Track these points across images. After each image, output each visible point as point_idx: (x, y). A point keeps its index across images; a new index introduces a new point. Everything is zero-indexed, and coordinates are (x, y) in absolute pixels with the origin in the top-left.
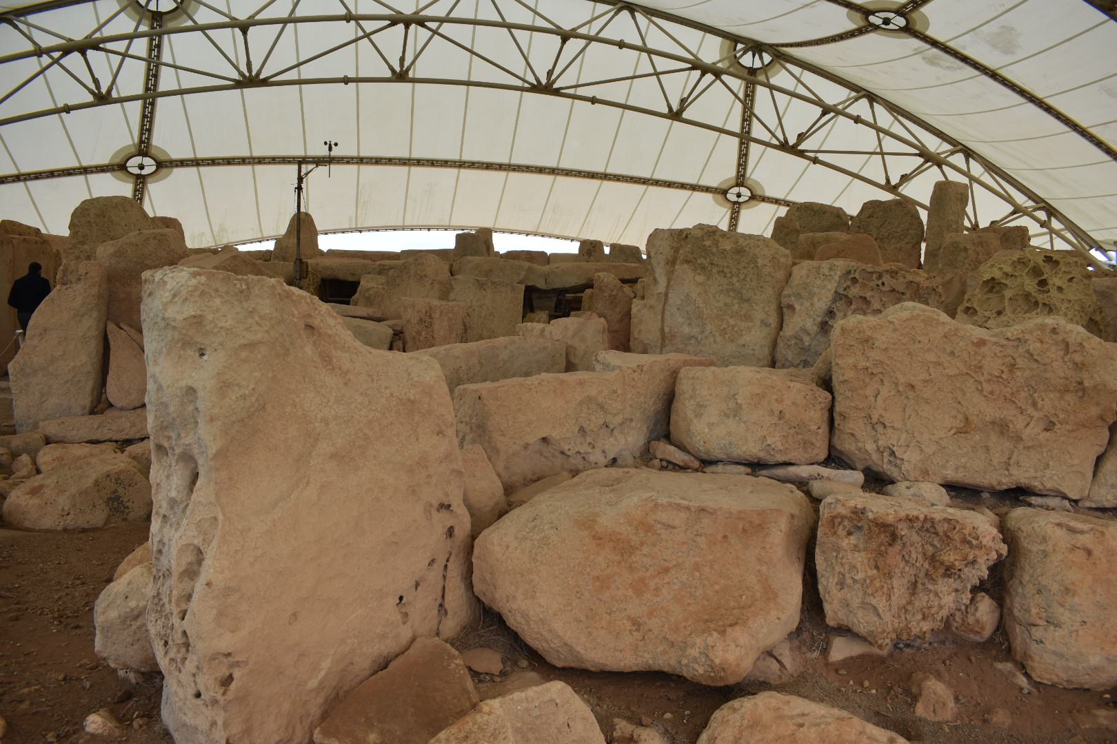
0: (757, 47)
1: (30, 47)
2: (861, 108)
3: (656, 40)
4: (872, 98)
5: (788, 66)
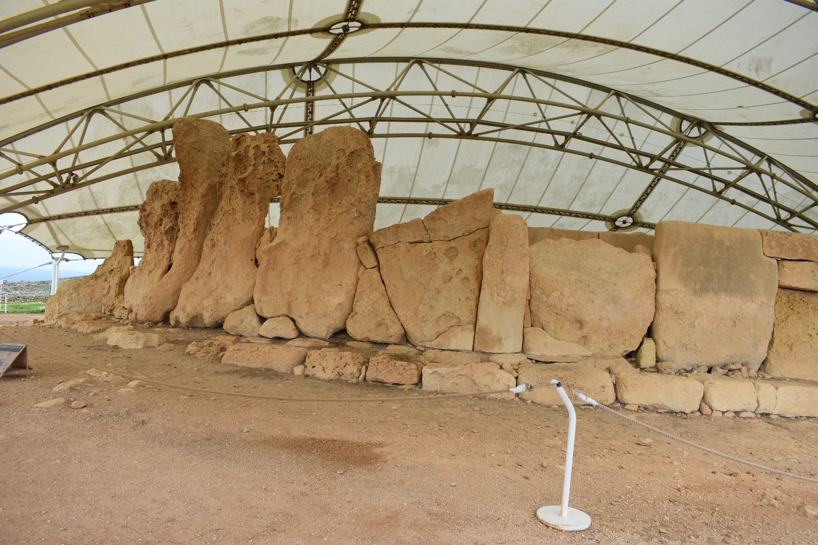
0: (700, 123)
4: (771, 161)
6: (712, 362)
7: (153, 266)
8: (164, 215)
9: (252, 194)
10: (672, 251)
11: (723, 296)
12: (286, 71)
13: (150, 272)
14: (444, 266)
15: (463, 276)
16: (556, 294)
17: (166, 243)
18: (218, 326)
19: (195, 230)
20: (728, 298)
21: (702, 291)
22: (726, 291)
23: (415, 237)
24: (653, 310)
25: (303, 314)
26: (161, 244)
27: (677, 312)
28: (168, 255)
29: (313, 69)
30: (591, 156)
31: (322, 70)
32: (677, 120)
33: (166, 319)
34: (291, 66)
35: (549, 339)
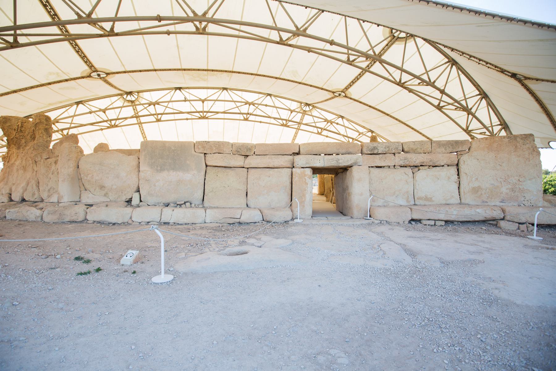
0: (307, 105)
1: (88, 111)
2: (340, 121)
3: (278, 104)
4: (342, 117)
5: (317, 110)
6: (167, 201)
10: (144, 153)
11: (172, 171)
16: (90, 176)
20: (174, 173)
21: (162, 170)
22: (173, 169)
24: (137, 180)
27: (146, 180)
30: (261, 122)
32: (299, 104)
35: (91, 195)
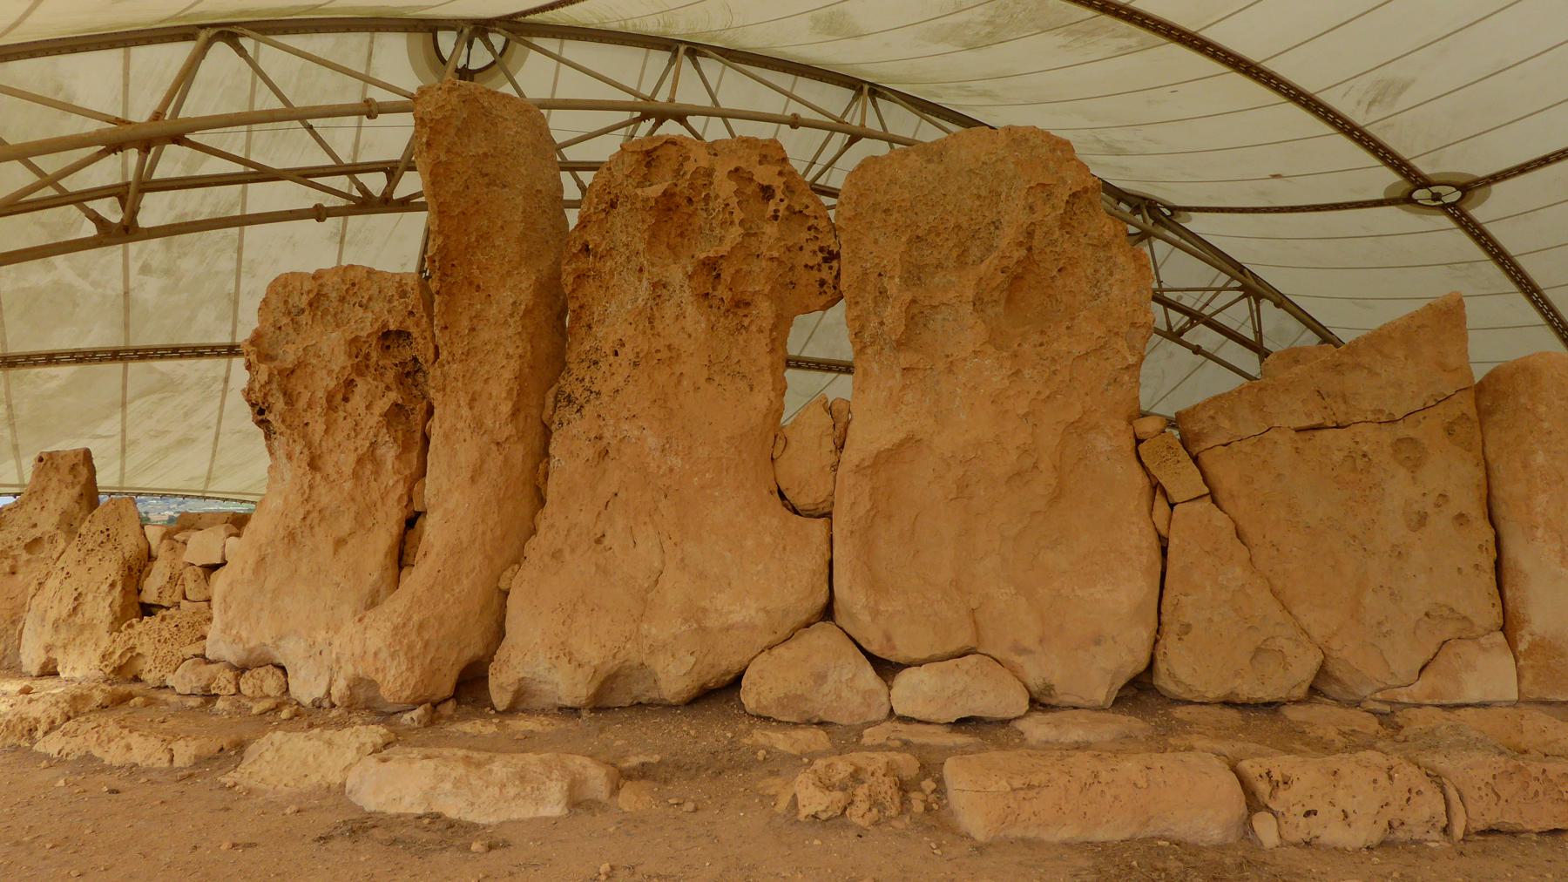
7: (345, 525)
8: (360, 370)
9: (741, 304)
12: (419, 38)
13: (340, 543)
14: (1399, 489)
15: (1452, 509)
17: (388, 453)
18: (720, 693)
19: (515, 413)
23: (1309, 415)
25: (1029, 641)
26: (369, 457)
28: (401, 489)
29: (478, 42)
31: (497, 40)
33: (470, 686)
34: (429, 27)
